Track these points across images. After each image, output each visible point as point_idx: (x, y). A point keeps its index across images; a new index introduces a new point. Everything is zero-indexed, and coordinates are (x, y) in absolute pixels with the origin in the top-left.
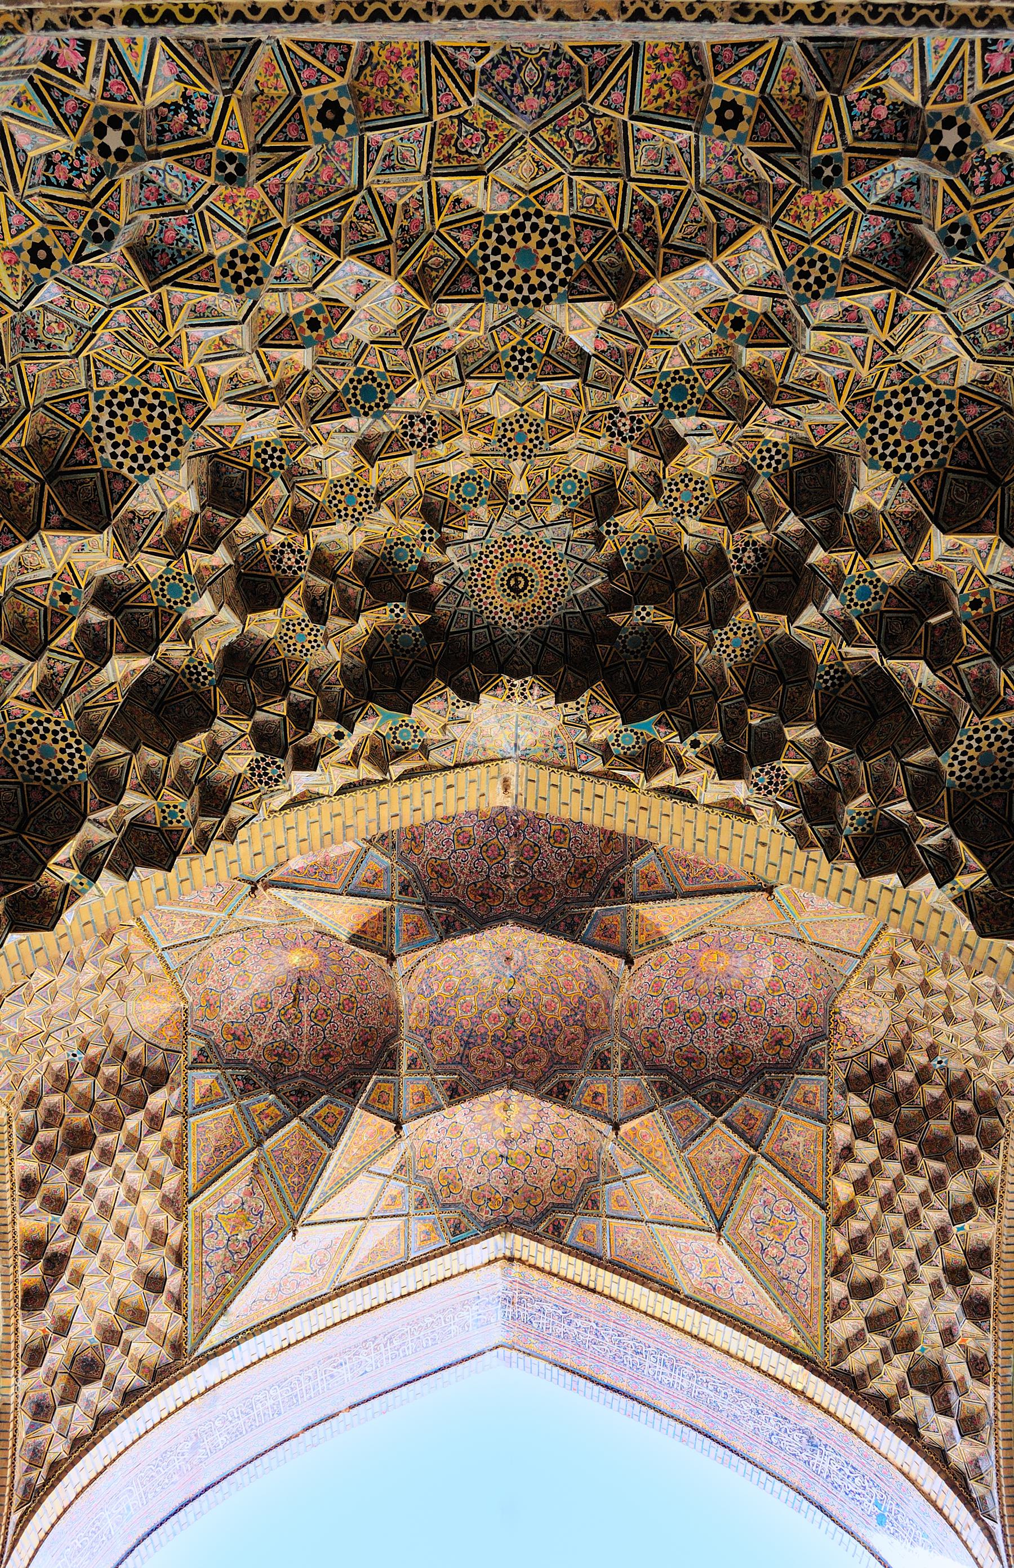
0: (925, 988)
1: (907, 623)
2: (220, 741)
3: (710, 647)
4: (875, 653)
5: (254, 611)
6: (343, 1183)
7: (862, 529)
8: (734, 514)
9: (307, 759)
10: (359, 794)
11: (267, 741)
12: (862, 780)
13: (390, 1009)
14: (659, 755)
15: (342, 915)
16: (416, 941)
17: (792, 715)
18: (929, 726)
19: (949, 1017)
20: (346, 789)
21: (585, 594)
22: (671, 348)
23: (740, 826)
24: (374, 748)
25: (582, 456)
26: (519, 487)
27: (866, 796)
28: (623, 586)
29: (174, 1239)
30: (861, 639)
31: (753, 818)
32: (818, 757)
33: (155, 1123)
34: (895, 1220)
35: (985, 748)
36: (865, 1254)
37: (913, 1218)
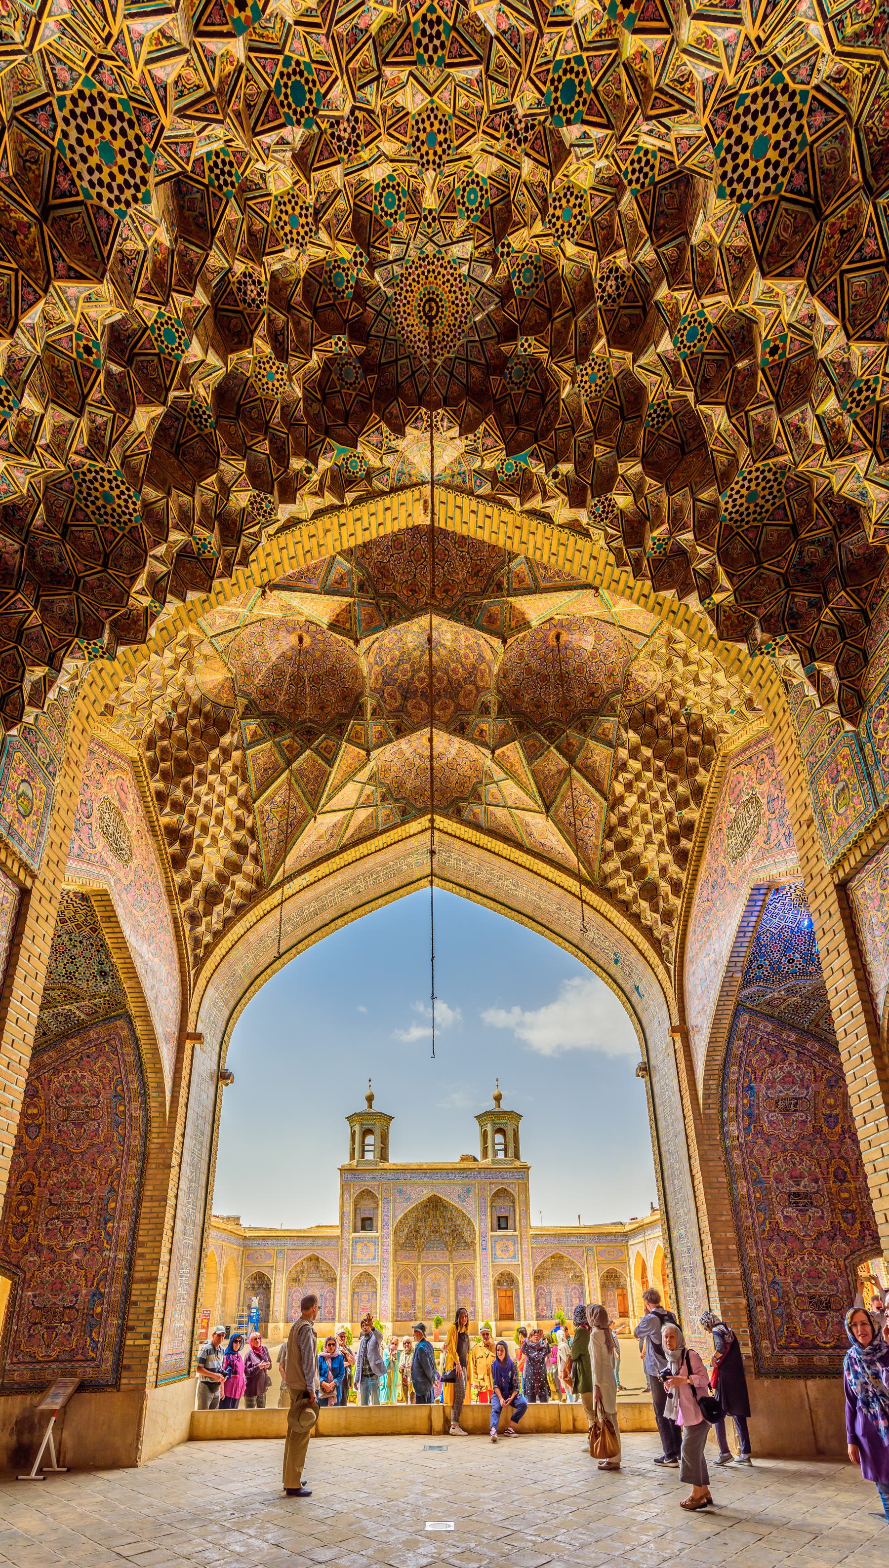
0: (687, 661)
1: (720, 366)
2: (226, 479)
3: (573, 383)
4: (691, 396)
5: (233, 351)
6: (339, 788)
7: (701, 265)
8: (603, 239)
9: (288, 494)
10: (326, 519)
11: (258, 478)
12: (665, 512)
13: (356, 673)
14: (530, 481)
15: (320, 609)
16: (372, 628)
17: (622, 451)
18: (719, 467)
19: (697, 682)
20: (318, 514)
21: (481, 321)
22: (564, 30)
23: (581, 543)
24: (333, 477)
25: (482, 159)
26: (430, 201)
27: (666, 526)
28: (513, 314)
29: (249, 823)
30: (683, 383)
31: (589, 536)
32: (638, 492)
33: (226, 753)
34: (646, 807)
35: (753, 488)
36: (627, 826)
37: (655, 806)
